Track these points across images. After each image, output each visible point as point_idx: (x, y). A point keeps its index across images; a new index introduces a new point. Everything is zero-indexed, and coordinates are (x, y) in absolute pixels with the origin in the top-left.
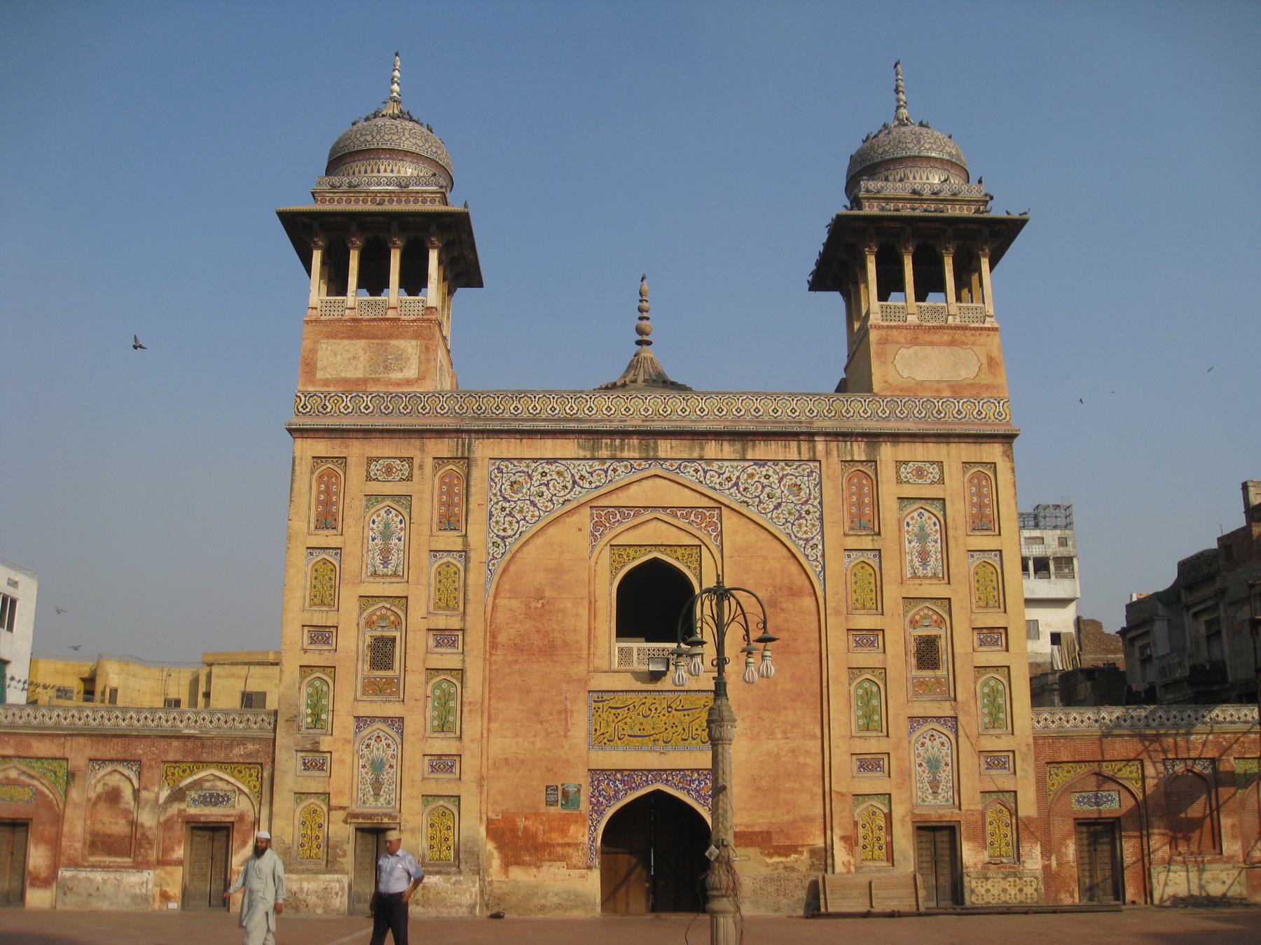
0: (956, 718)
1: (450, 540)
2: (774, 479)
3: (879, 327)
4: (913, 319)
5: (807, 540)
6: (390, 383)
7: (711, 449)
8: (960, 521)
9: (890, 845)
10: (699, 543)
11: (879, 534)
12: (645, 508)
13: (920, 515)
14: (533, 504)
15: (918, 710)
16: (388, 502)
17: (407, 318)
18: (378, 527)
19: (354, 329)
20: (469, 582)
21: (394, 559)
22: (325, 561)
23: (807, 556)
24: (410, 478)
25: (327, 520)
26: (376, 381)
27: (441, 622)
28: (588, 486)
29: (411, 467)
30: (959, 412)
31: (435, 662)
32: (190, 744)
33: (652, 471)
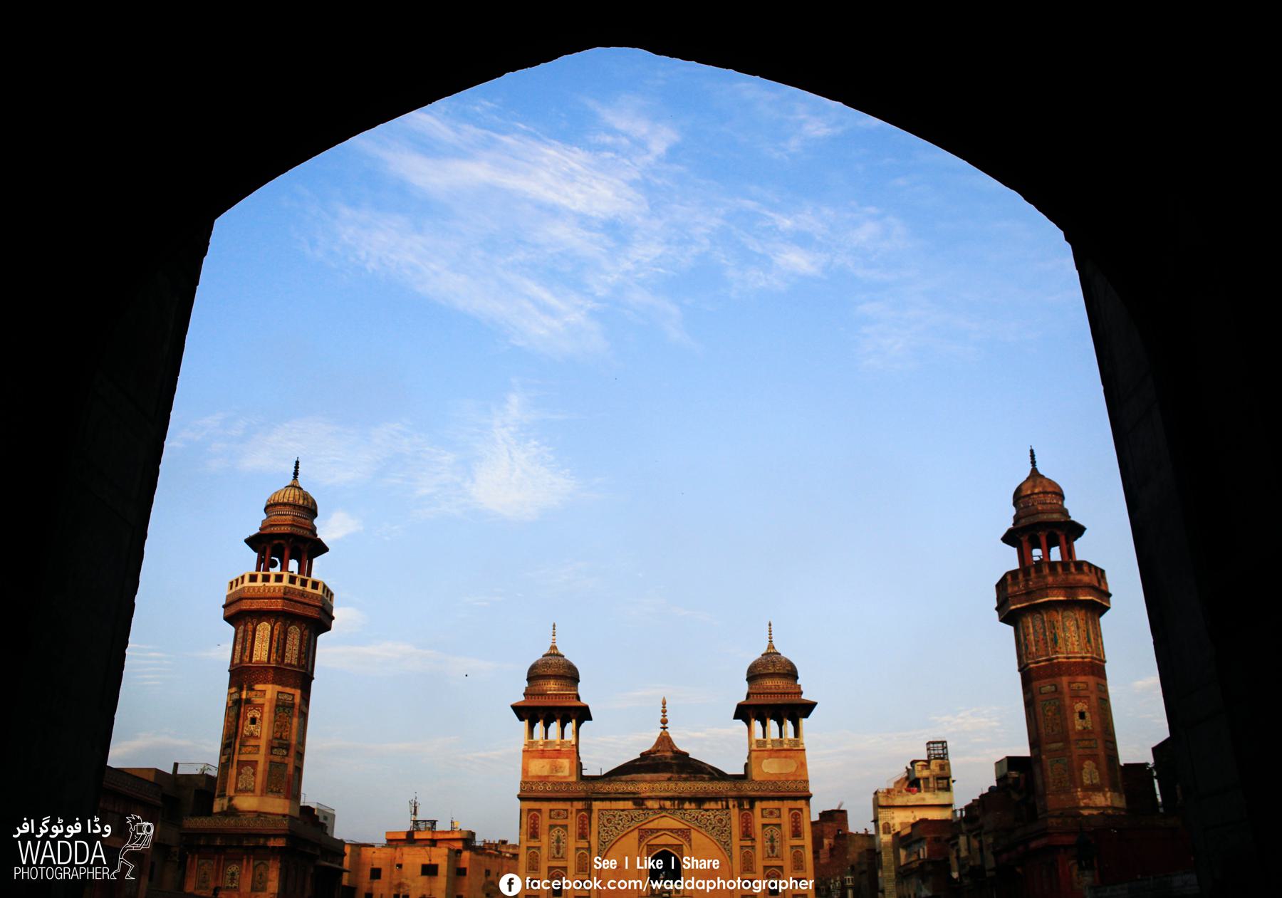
1: (584, 844)
2: (712, 817)
3: (755, 751)
4: (769, 747)
5: (725, 842)
6: (558, 777)
7: (687, 805)
12: (661, 829)
13: (771, 831)
14: (616, 828)
16: (558, 828)
18: (555, 838)
19: (542, 754)
21: (561, 851)
22: (534, 852)
23: (725, 849)
24: (567, 818)
30: (788, 787)
33: (663, 814)
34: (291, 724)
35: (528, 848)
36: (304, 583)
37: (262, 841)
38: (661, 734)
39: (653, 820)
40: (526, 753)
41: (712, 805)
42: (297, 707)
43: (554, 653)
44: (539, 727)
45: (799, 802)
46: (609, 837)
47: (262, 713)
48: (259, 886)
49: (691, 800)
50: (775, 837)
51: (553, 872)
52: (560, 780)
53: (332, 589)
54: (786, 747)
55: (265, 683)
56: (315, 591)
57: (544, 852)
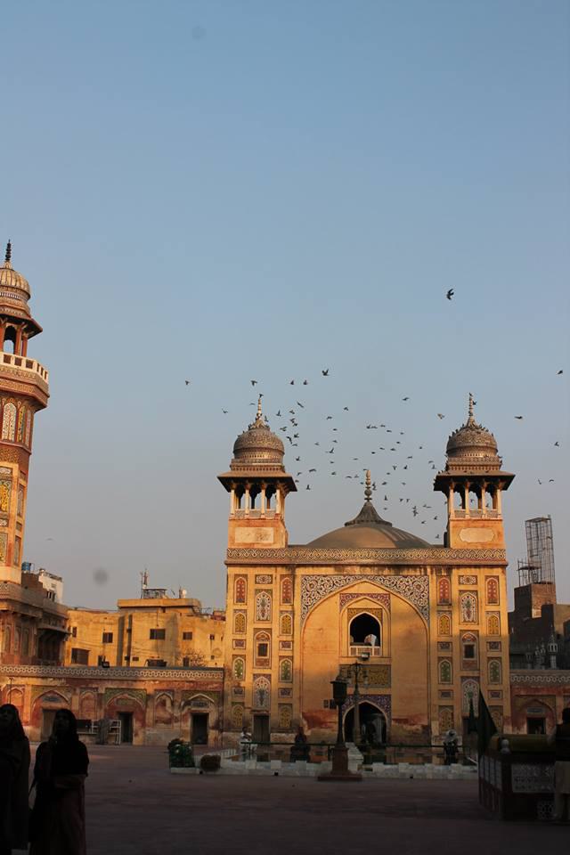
0: (479, 677)
1: (287, 607)
4: (468, 517)
7: (386, 572)
8: (483, 600)
9: (453, 725)
10: (380, 607)
11: (451, 605)
15: (465, 674)
18: (260, 602)
19: (248, 523)
21: (266, 614)
24: (271, 583)
25: (241, 598)
27: (284, 638)
31: (283, 653)
32: (192, 684)
35: (235, 611)
36: (18, 362)
38: (365, 505)
39: (353, 586)
40: (232, 522)
41: (411, 572)
42: (15, 479)
44: (246, 496)
45: (495, 570)
49: (390, 566)
50: (472, 602)
52: (265, 548)
54: (483, 518)
56: (29, 370)
57: (251, 615)
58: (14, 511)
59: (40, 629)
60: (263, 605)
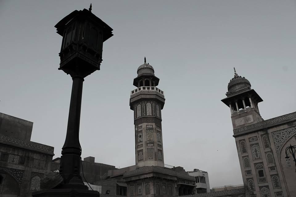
1: (268, 150)
14: (282, 139)
17: (248, 111)
18: (254, 150)
19: (240, 116)
20: (274, 156)
22: (246, 158)
24: (257, 140)
26: (246, 124)
28: (292, 132)
29: (257, 137)
34: (153, 135)
36: (148, 88)
37: (146, 176)
43: (236, 77)
46: (280, 144)
47: (142, 133)
48: (148, 193)
51: (256, 166)
52: (250, 124)
53: (161, 89)
55: (142, 123)
57: (251, 157)
58: (156, 140)
59: (178, 185)
60: (256, 151)
